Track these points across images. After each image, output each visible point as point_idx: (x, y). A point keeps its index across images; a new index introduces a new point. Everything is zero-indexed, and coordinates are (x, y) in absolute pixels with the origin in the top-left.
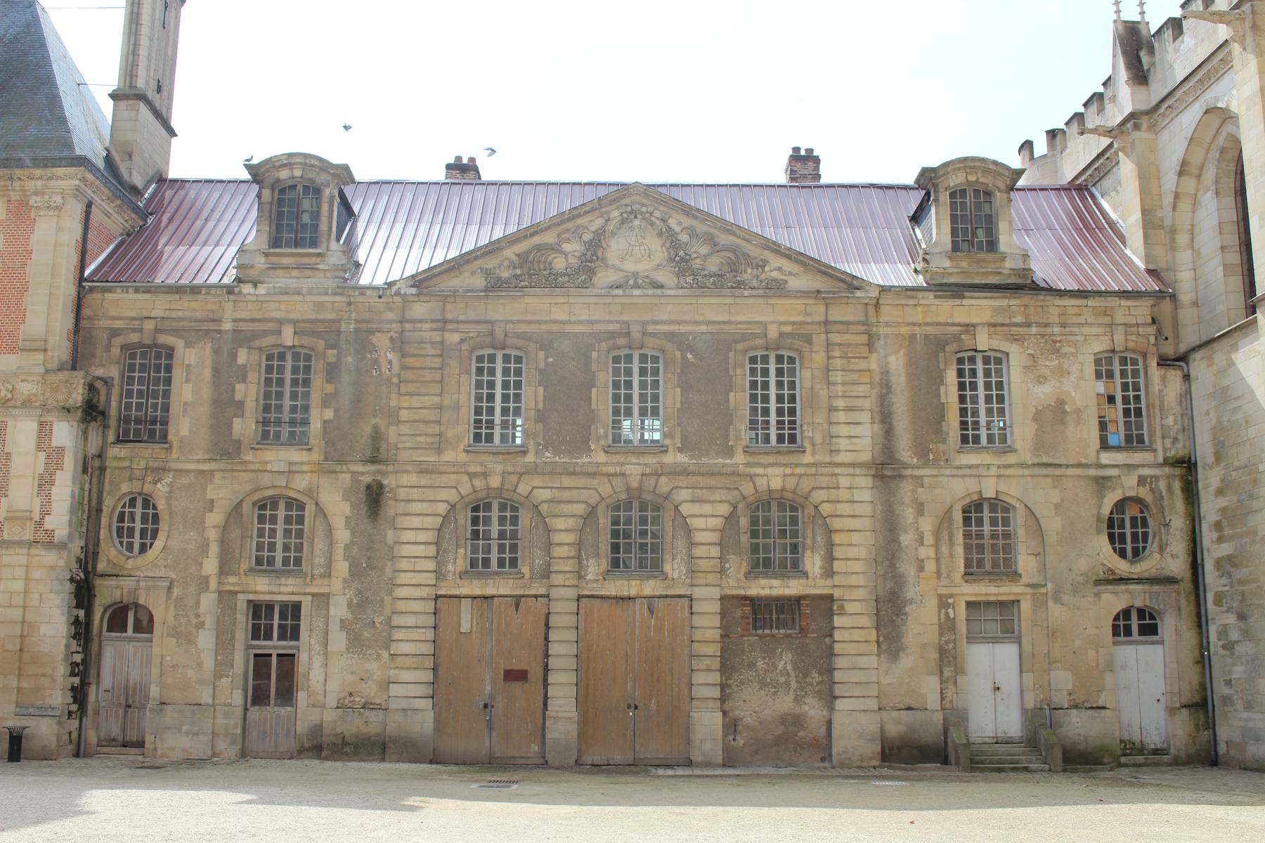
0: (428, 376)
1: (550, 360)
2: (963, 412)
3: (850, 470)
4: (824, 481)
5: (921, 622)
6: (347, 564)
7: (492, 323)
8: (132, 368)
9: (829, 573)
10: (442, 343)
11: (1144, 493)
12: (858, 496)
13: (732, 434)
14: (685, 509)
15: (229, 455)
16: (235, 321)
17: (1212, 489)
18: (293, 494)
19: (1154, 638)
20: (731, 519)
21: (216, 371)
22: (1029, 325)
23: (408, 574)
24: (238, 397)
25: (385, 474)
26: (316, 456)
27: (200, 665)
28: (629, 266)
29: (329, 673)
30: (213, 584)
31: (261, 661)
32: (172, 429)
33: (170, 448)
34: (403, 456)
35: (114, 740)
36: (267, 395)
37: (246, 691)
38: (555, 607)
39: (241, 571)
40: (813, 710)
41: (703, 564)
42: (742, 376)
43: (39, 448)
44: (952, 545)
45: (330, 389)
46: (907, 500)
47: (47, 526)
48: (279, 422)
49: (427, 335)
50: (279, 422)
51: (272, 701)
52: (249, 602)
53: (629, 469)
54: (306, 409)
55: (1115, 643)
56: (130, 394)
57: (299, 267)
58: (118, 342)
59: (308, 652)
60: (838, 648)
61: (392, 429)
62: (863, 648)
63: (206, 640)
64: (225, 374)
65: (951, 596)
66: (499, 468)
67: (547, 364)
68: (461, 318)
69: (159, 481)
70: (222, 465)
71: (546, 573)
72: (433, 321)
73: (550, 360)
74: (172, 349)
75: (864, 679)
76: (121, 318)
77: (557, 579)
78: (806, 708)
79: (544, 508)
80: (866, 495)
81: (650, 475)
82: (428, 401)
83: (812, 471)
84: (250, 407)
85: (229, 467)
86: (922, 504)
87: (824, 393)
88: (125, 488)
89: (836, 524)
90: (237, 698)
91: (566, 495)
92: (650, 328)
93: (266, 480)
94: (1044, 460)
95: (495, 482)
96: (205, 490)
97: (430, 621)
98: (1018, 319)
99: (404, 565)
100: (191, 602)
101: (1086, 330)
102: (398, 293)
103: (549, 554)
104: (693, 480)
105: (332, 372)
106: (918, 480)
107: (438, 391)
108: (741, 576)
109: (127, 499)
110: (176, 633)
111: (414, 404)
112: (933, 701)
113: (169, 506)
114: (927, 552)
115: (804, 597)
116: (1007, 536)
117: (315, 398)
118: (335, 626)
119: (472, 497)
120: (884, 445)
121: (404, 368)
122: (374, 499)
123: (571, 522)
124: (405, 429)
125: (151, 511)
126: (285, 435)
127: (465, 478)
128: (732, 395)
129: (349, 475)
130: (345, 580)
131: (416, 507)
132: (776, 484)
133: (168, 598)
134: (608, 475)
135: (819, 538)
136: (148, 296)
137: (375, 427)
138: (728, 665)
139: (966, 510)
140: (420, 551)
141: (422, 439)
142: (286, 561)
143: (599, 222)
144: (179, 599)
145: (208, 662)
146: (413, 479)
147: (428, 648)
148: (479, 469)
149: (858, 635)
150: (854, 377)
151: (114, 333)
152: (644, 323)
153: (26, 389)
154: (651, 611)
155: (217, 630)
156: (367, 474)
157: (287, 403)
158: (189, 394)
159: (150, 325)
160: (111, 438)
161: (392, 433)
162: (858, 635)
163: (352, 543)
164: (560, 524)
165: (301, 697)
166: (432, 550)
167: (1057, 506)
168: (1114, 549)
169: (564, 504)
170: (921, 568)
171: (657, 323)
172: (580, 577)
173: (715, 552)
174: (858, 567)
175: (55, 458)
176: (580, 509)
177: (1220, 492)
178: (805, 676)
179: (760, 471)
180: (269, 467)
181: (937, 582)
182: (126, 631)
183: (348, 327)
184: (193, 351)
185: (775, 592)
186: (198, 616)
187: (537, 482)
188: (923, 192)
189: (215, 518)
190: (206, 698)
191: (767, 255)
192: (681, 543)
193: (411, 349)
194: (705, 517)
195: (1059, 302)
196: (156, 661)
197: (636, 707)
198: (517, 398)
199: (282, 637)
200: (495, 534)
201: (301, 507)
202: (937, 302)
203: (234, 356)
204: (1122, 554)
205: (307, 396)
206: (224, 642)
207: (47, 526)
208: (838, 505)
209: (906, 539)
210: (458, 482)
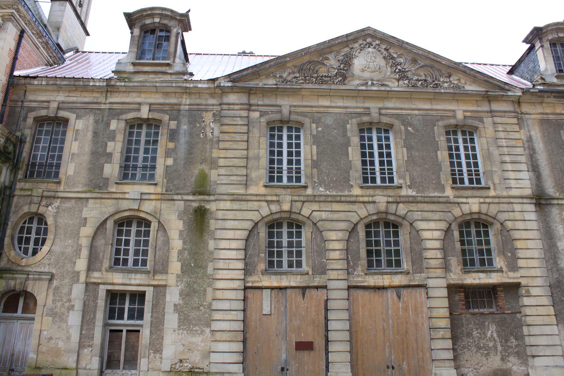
0: (238, 137)
1: (320, 129)
3: (520, 200)
4: (505, 207)
6: (179, 264)
8: (40, 133)
12: (528, 216)
13: (442, 176)
15: (100, 188)
18: (143, 215)
20: (448, 231)
21: (96, 134)
23: (224, 272)
24: (109, 150)
25: (209, 201)
27: (69, 338)
28: (367, 75)
30: (82, 278)
31: (115, 333)
32: (62, 170)
33: (59, 183)
36: (129, 151)
37: (102, 357)
38: (333, 295)
39: (103, 269)
45: (171, 145)
48: (135, 167)
50: (135, 167)
51: (121, 366)
52: (108, 291)
53: (377, 199)
54: (154, 159)
58: (32, 115)
62: (547, 320)
63: (74, 319)
64: (101, 136)
66: (289, 198)
67: (318, 132)
69: (50, 205)
72: (241, 104)
73: (320, 129)
75: (550, 343)
77: (333, 275)
78: (511, 365)
80: (533, 216)
81: (392, 202)
82: (238, 153)
83: (497, 200)
85: (99, 195)
87: (496, 152)
88: (26, 209)
91: (335, 216)
92: (383, 111)
93: (125, 205)
95: (286, 207)
96: (82, 211)
97: (240, 306)
100: (65, 290)
102: (219, 87)
105: (173, 135)
107: (245, 147)
109: (27, 218)
110: (53, 314)
113: (56, 222)
120: (537, 185)
122: (199, 219)
123: (340, 235)
124: (222, 171)
125: (43, 226)
127: (265, 204)
128: (439, 153)
129: (183, 202)
130: (178, 276)
133: (48, 288)
134: (364, 202)
138: (456, 334)
140: (233, 254)
141: (234, 178)
144: (57, 288)
147: (239, 326)
148: (274, 198)
149: (542, 311)
150: (513, 143)
152: (380, 109)
154: (399, 297)
155: (84, 312)
156: (195, 201)
157: (141, 155)
158: (76, 147)
159: (54, 105)
161: (213, 175)
162: (542, 311)
163: (184, 249)
164: (333, 235)
166: (241, 255)
169: (335, 220)
171: (387, 109)
173: (439, 254)
178: (507, 341)
179: (464, 200)
180: (127, 196)
182: (16, 312)
184: (81, 121)
186: (70, 300)
187: (315, 207)
188: (529, 45)
189: (87, 231)
193: (226, 121)
194: (431, 232)
196: (36, 334)
197: (393, 368)
198: (298, 154)
199: (131, 317)
200: (285, 244)
201: (148, 224)
203: (108, 125)
205: (155, 151)
208: (516, 223)
210: (260, 207)
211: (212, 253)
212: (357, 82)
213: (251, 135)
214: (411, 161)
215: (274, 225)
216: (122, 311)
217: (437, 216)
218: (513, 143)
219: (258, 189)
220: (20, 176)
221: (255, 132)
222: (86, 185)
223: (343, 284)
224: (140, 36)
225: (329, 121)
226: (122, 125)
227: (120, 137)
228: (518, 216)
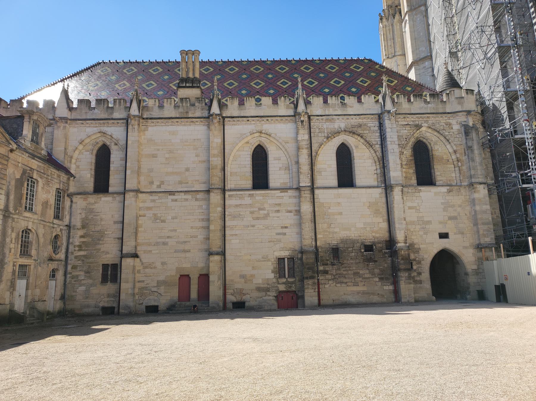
17: (78, 236)
46: (10, 226)
55: (50, 280)
94: (42, 219)
98: (42, 171)
106: (13, 219)
170: (10, 252)
177: (82, 237)
209: (8, 240)
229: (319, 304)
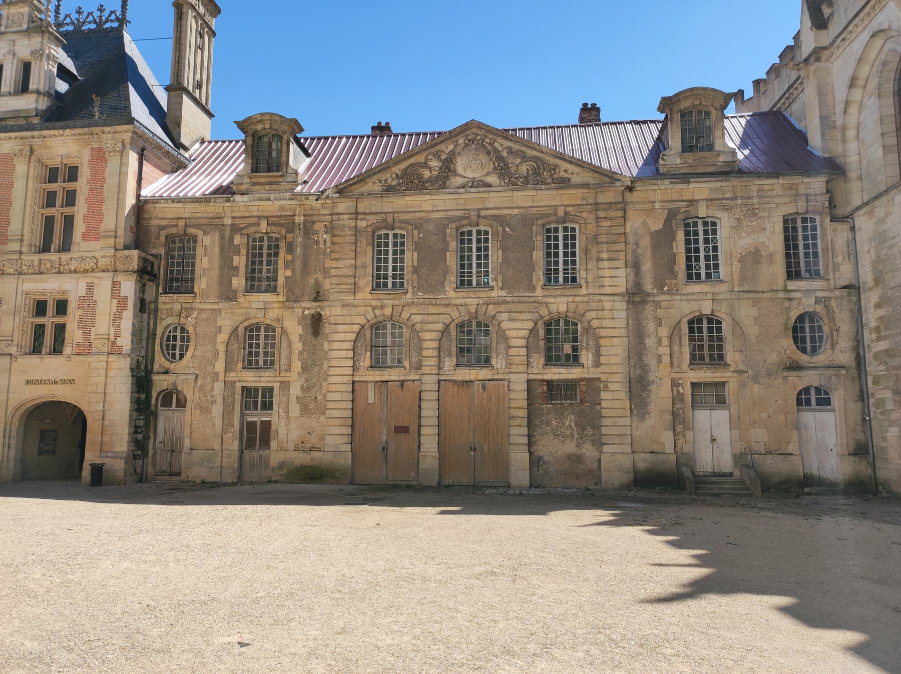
2: (688, 259)
3: (612, 298)
4: (594, 305)
5: (660, 395)
6: (300, 363)
7: (386, 213)
9: (597, 364)
10: (356, 227)
11: (819, 308)
14: (504, 325)
16: (233, 218)
17: (872, 305)
18: (268, 322)
19: (828, 407)
20: (533, 331)
21: (222, 248)
22: (735, 198)
24: (235, 264)
26: (281, 298)
27: (214, 426)
28: (470, 174)
29: (289, 429)
34: (332, 297)
35: (164, 472)
36: (253, 263)
37: (241, 440)
38: (425, 387)
40: (588, 451)
41: (516, 360)
42: (539, 241)
43: (112, 297)
44: (681, 345)
45: (289, 257)
46: (650, 317)
47: (118, 344)
48: (260, 280)
49: (347, 222)
52: (243, 387)
56: (172, 265)
57: (270, 183)
58: (163, 233)
59: (276, 417)
60: (604, 412)
61: (327, 281)
62: (621, 412)
63: (217, 410)
64: (227, 251)
65: (680, 379)
67: (419, 238)
68: (367, 211)
70: (226, 305)
71: (419, 367)
74: (196, 237)
76: (165, 219)
77: (426, 370)
79: (418, 326)
80: (623, 314)
83: (586, 298)
84: (242, 270)
86: (660, 319)
88: (170, 320)
89: (603, 333)
90: (235, 445)
91: (431, 318)
92: (483, 213)
94: (746, 288)
98: (728, 195)
99: (334, 363)
100: (208, 388)
101: (777, 200)
103: (420, 354)
104: (509, 306)
105: (290, 249)
106: (658, 305)
108: (540, 366)
109: (171, 328)
110: (199, 406)
111: (339, 266)
112: (669, 448)
114: (664, 350)
115: (582, 380)
116: (720, 339)
117: (281, 263)
118: (293, 400)
119: (375, 320)
121: (333, 243)
122: (316, 323)
124: (334, 280)
126: (263, 287)
127: (370, 309)
128: (534, 253)
130: (299, 373)
131: (341, 328)
132: (563, 308)
134: (456, 305)
135: (591, 342)
136: (181, 205)
137: (317, 280)
139: (690, 322)
140: (343, 354)
141: (344, 286)
142: (265, 362)
143: (451, 147)
145: (218, 423)
146: (338, 310)
147: (348, 414)
149: (618, 404)
151: (162, 228)
152: (479, 210)
153: (103, 262)
156: (309, 308)
157: (265, 267)
158: (206, 265)
160: (161, 291)
161: (327, 284)
162: (618, 404)
163: (303, 350)
164: (427, 336)
165: (273, 444)
166: (350, 354)
167: (755, 319)
168: (798, 348)
170: (660, 360)
171: (487, 209)
172: (440, 369)
173: (524, 351)
174: (617, 360)
175: (122, 303)
176: (440, 327)
177: (878, 306)
178: (583, 430)
180: (254, 306)
181: (672, 369)
183: (299, 219)
185: (562, 377)
187: (413, 310)
189: (222, 338)
190: (217, 447)
191: (557, 161)
192: (502, 347)
193: (336, 232)
194: (517, 329)
195: (759, 182)
196: (188, 424)
198: (402, 260)
201: (274, 330)
202: (671, 186)
203: (232, 239)
204: (804, 351)
206: (227, 411)
207: (118, 344)
209: (650, 342)
210: (366, 312)
211: (326, 353)
212: (459, 181)
213: (358, 244)
214: (505, 261)
215: (377, 327)
216: (256, 403)
217: (524, 317)
218: (614, 238)
219: (365, 294)
220: (161, 291)
221: (363, 242)
222: (218, 297)
223: (435, 378)
224: (253, 145)
225: (431, 227)
226: (245, 239)
227: (243, 252)
228: (606, 314)
229: (240, 480)
